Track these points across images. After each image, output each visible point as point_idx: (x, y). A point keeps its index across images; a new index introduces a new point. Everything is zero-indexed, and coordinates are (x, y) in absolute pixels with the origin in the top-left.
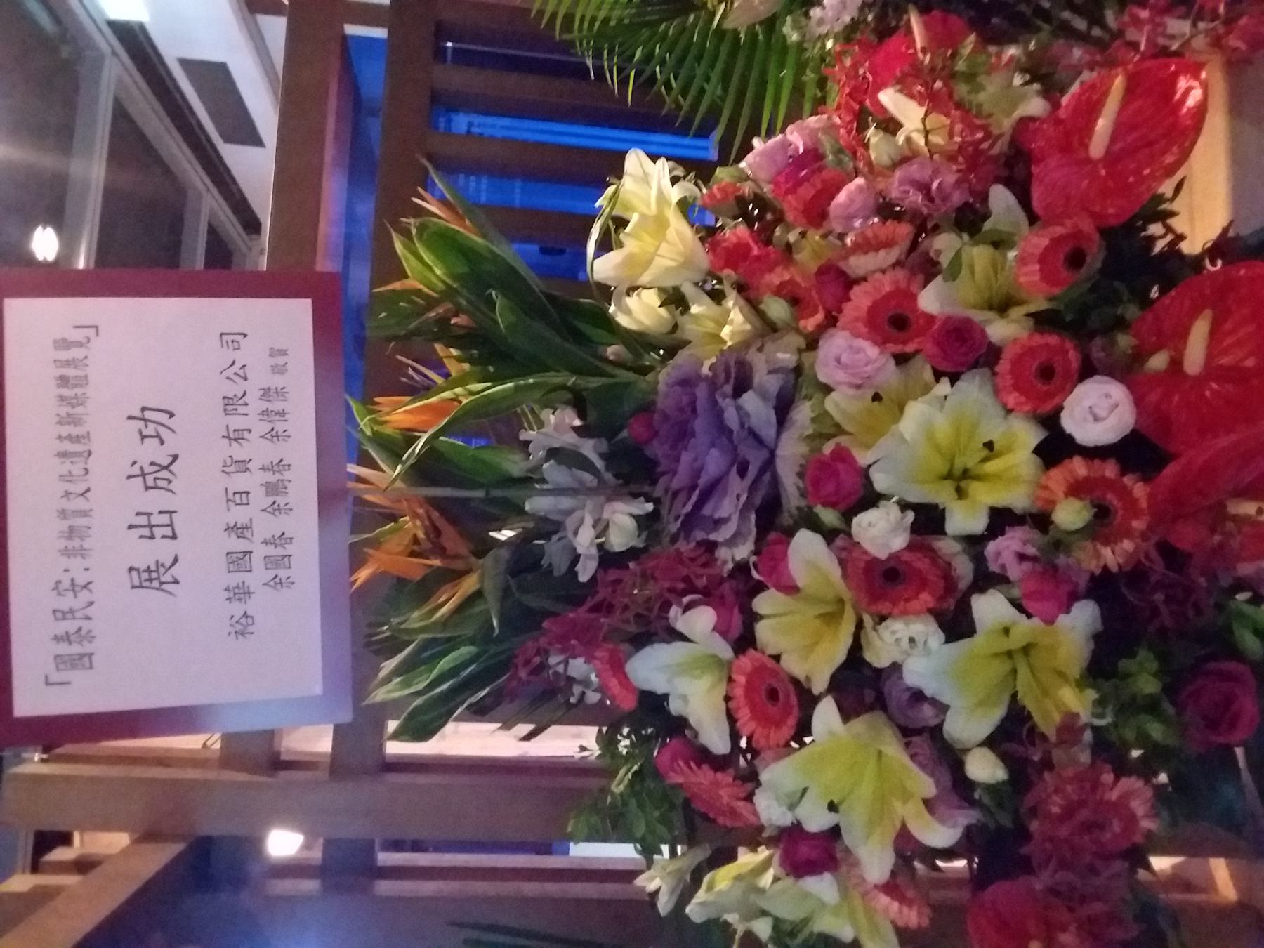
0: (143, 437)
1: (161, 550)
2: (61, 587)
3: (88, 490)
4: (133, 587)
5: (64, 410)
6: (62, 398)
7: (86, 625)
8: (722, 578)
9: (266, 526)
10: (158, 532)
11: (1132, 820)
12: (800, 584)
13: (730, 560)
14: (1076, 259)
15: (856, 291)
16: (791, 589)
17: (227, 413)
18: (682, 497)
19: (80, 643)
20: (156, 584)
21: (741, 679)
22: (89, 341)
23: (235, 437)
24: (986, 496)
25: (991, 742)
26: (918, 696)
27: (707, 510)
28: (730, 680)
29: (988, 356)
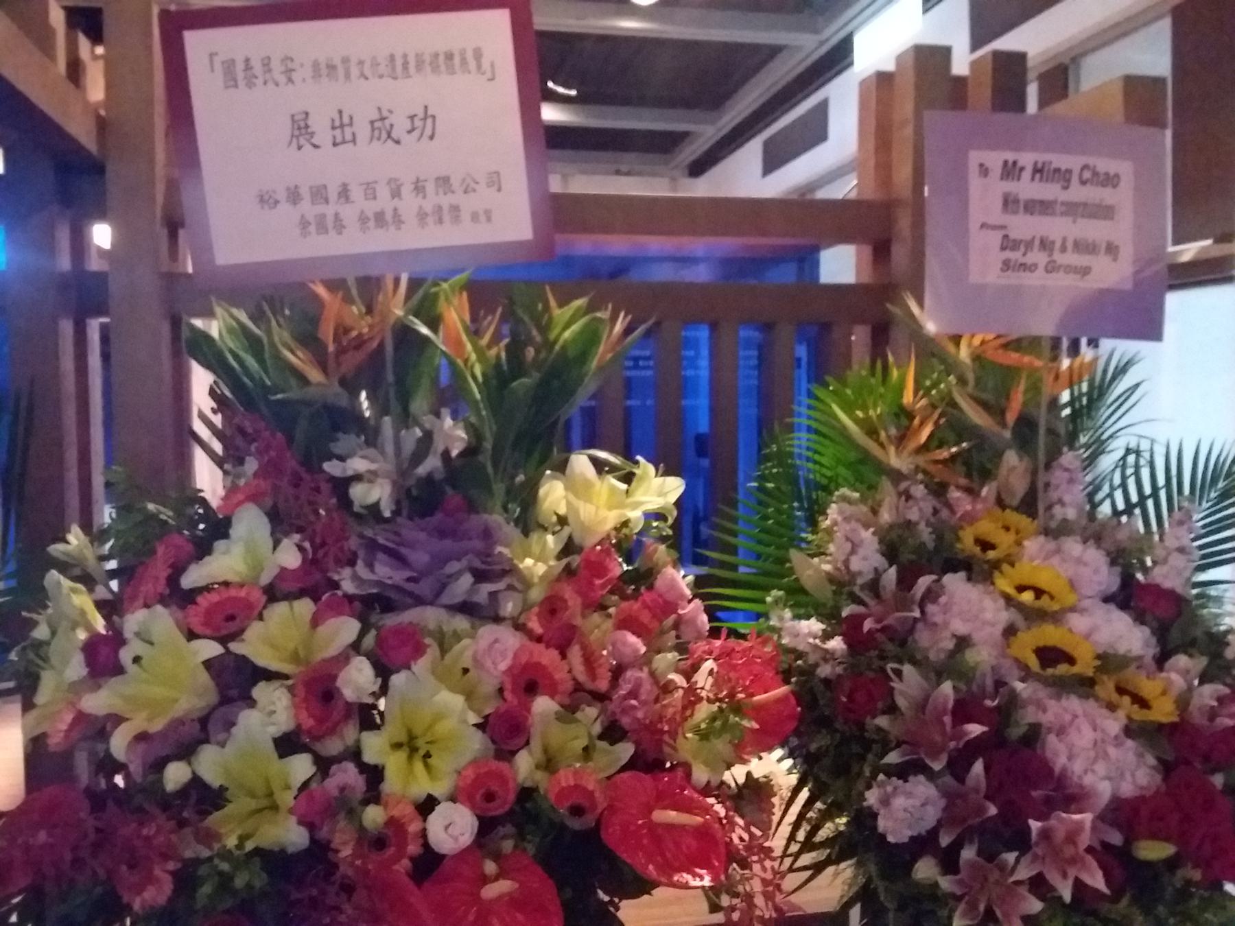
0: (412, 118)
1: (323, 135)
2: (289, 62)
3: (367, 78)
5: (427, 58)
6: (436, 55)
7: (259, 82)
8: (327, 571)
9: (349, 213)
10: (338, 132)
11: (139, 889)
12: (321, 629)
13: (341, 577)
14: (577, 811)
15: (554, 654)
16: (316, 621)
17: (438, 179)
18: (392, 537)
19: (245, 78)
20: (296, 133)
21: (243, 593)
22: (483, 74)
23: (419, 188)
24: (394, 764)
25: (196, 781)
26: (230, 724)
27: (381, 556)
28: (242, 586)
29: (506, 754)
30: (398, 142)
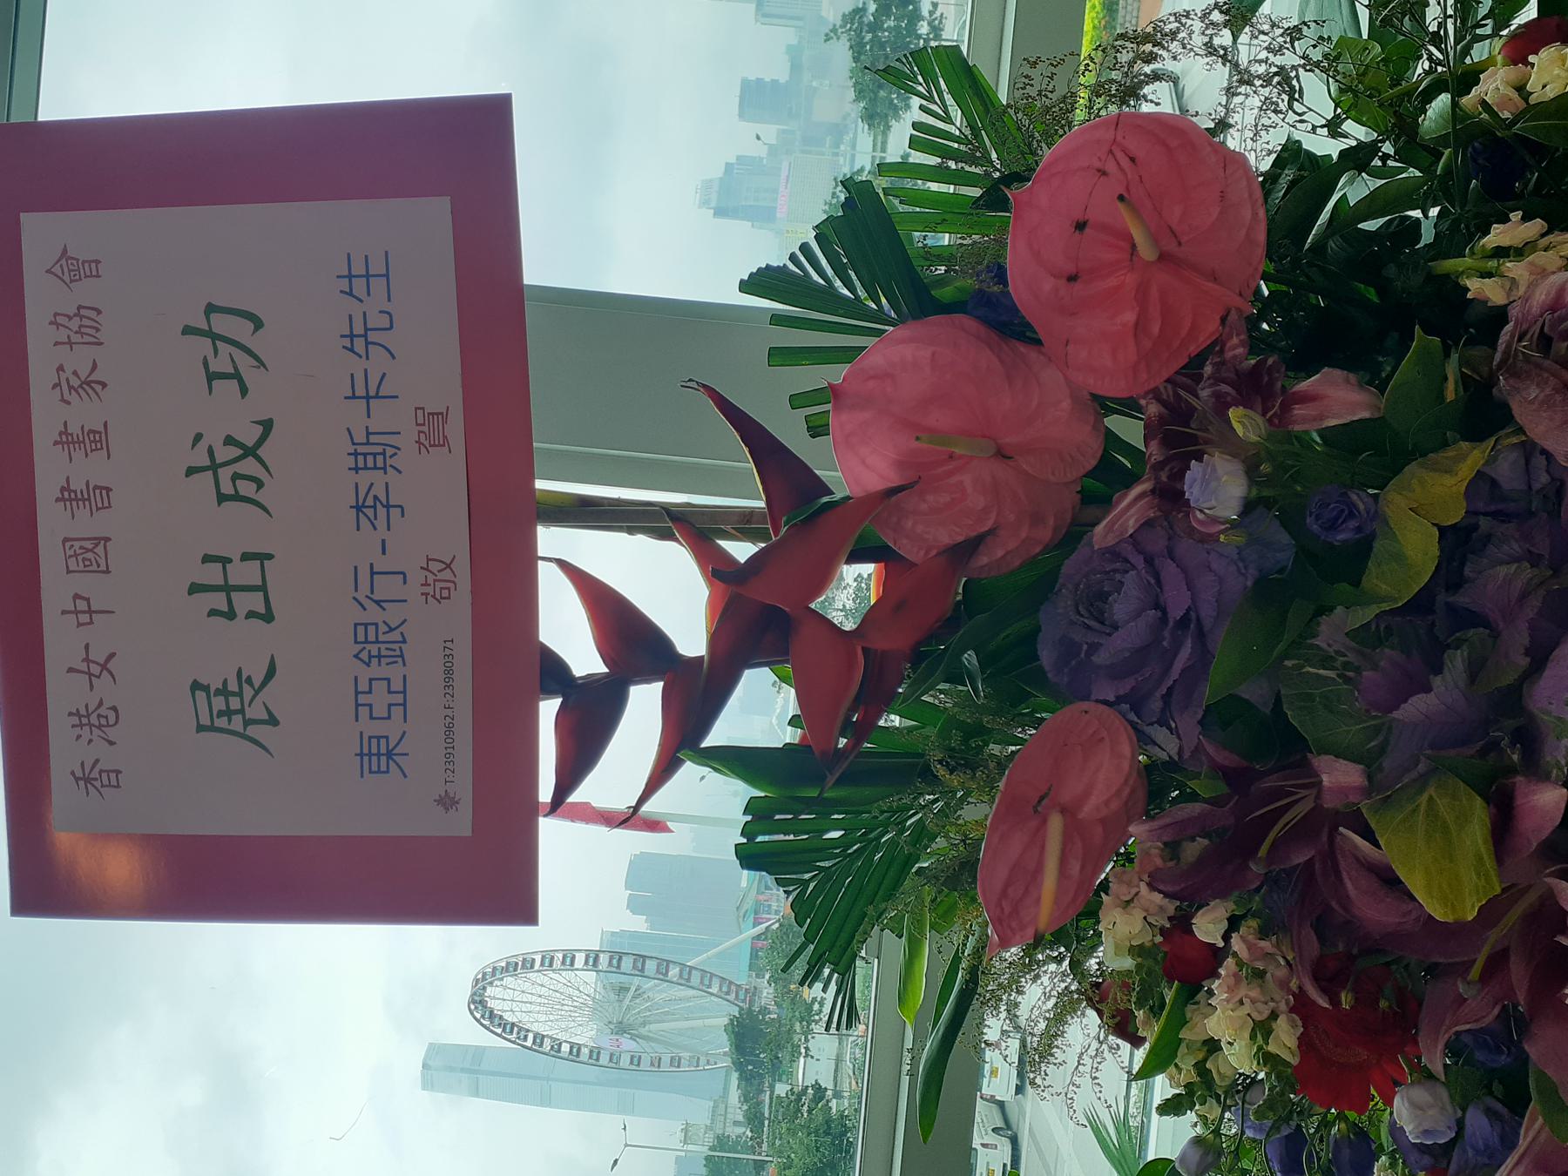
4: (200, 728)
30: (267, 425)
